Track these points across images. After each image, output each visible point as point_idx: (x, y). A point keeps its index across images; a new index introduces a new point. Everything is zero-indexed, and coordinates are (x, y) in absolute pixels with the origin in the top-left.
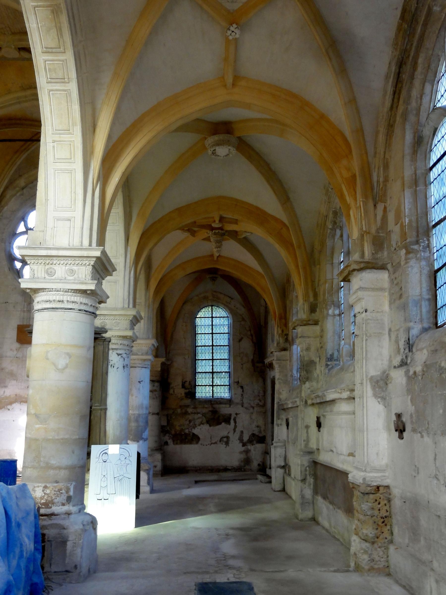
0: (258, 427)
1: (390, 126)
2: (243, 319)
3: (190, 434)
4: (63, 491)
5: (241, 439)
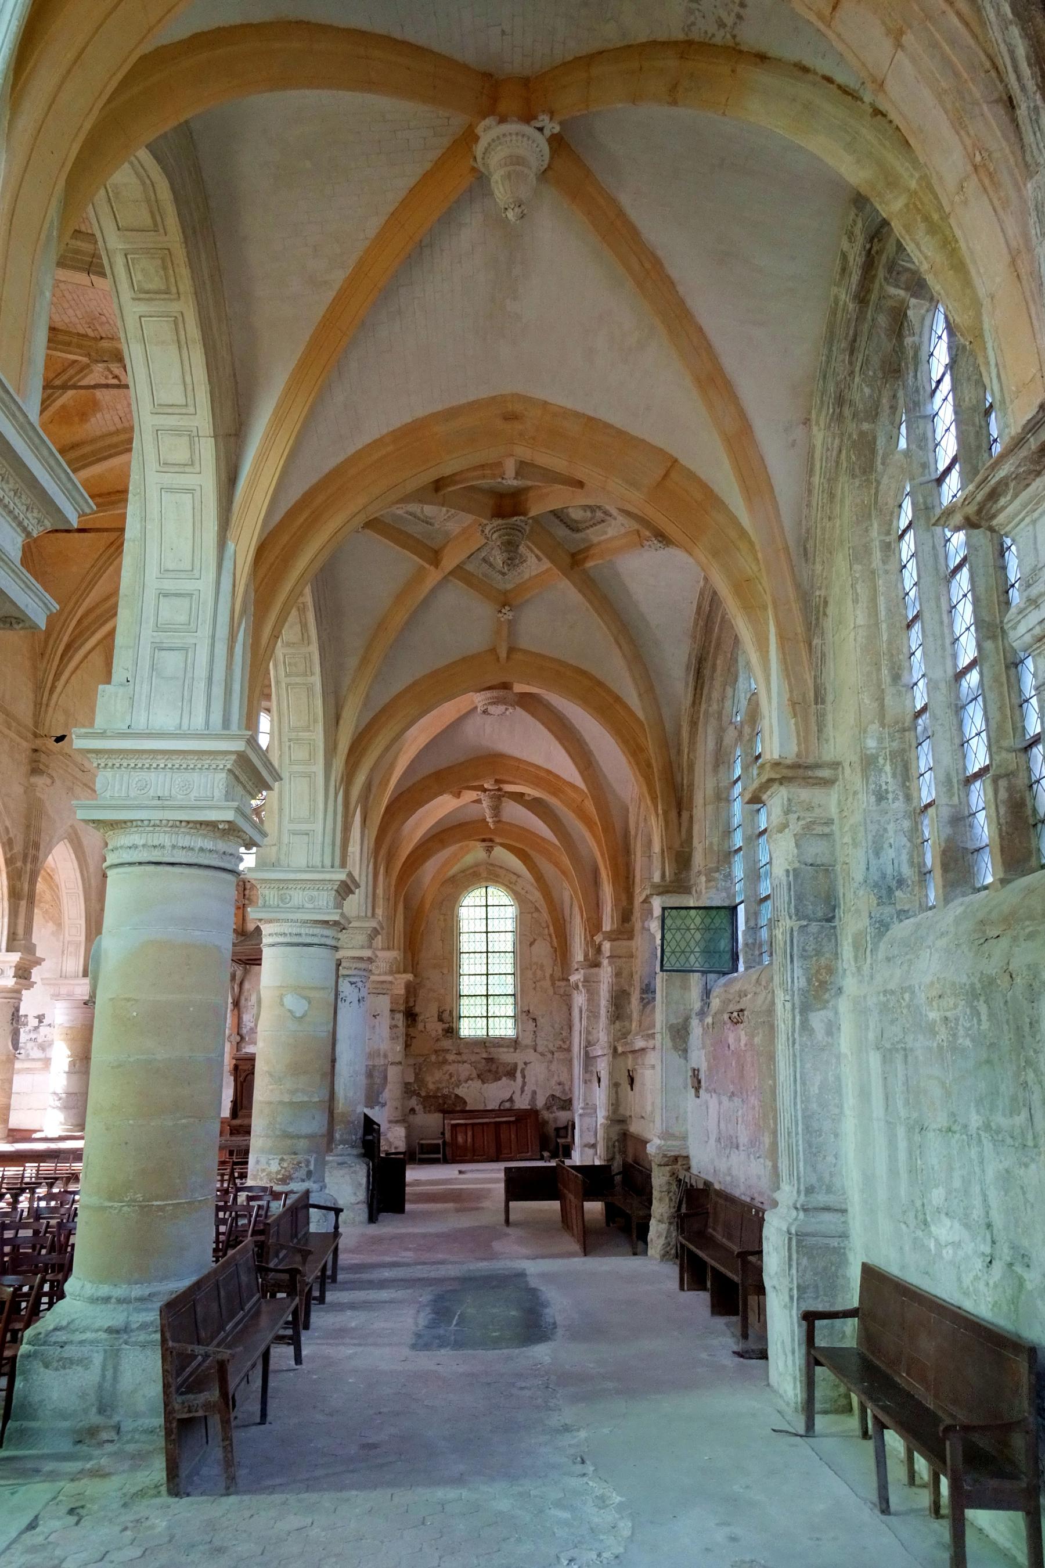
0: (559, 1084)
1: (694, 724)
4: (303, 1165)
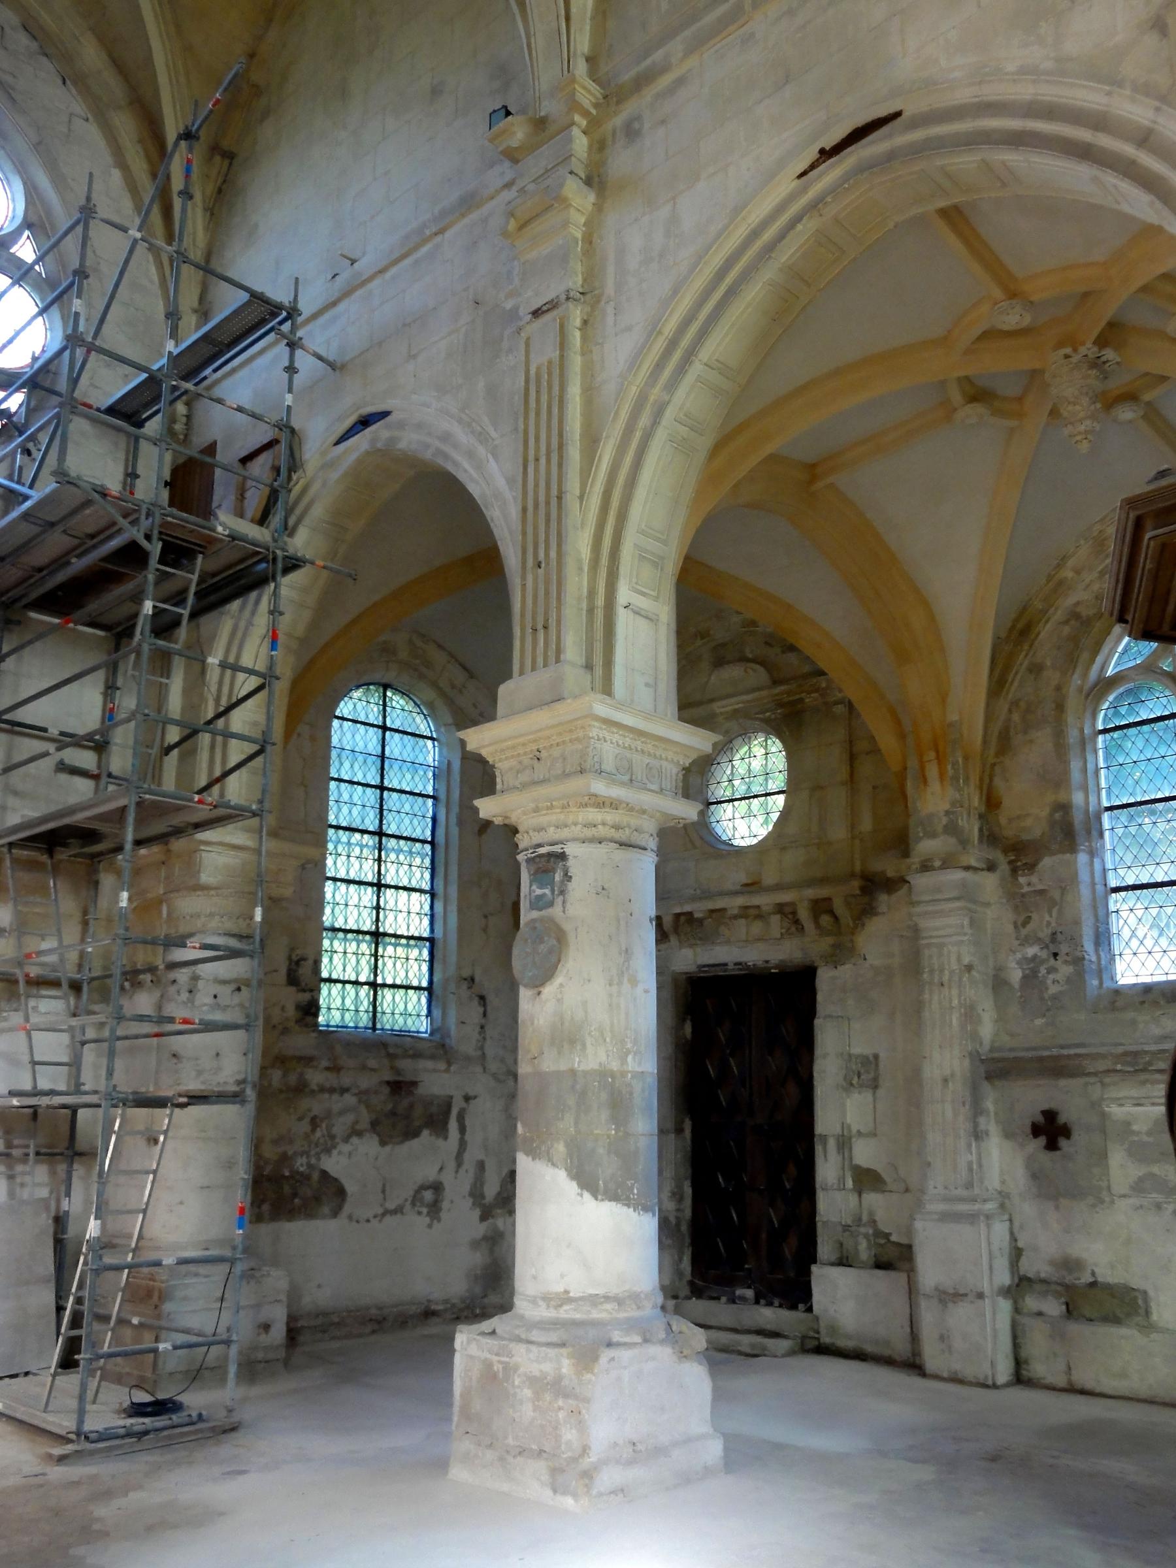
3: (308, 1178)
5: (476, 1194)
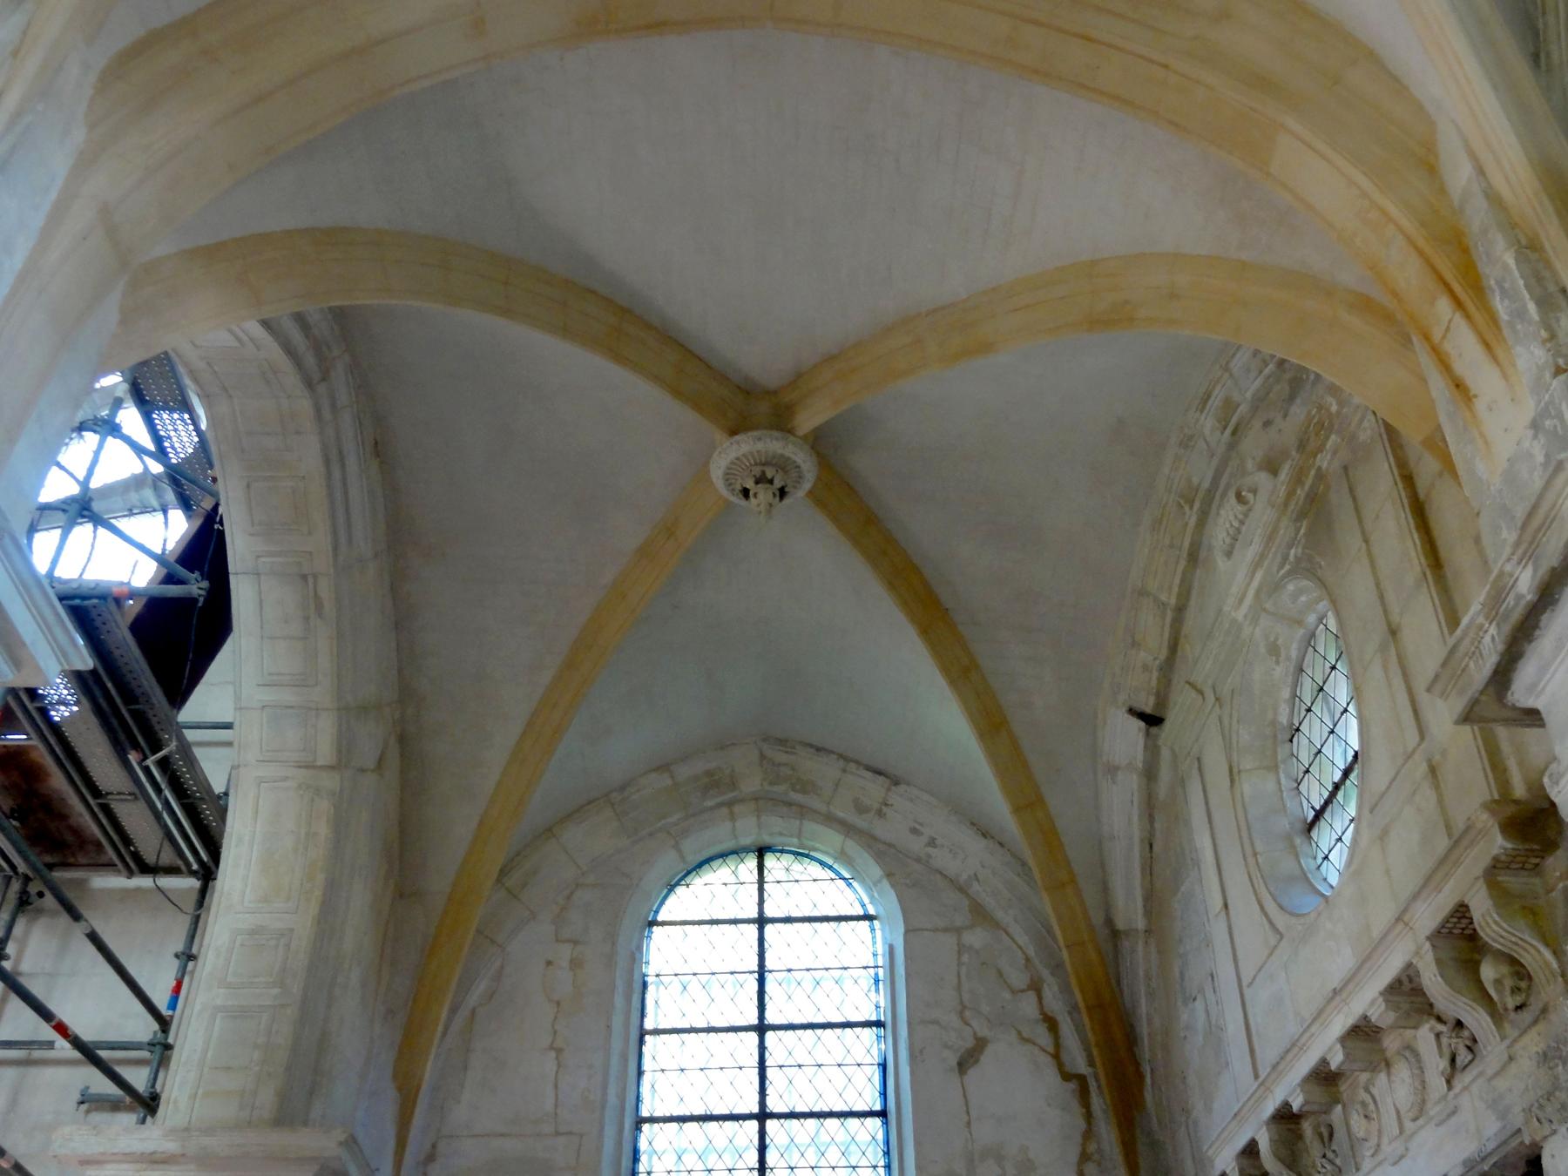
2: (980, 914)
